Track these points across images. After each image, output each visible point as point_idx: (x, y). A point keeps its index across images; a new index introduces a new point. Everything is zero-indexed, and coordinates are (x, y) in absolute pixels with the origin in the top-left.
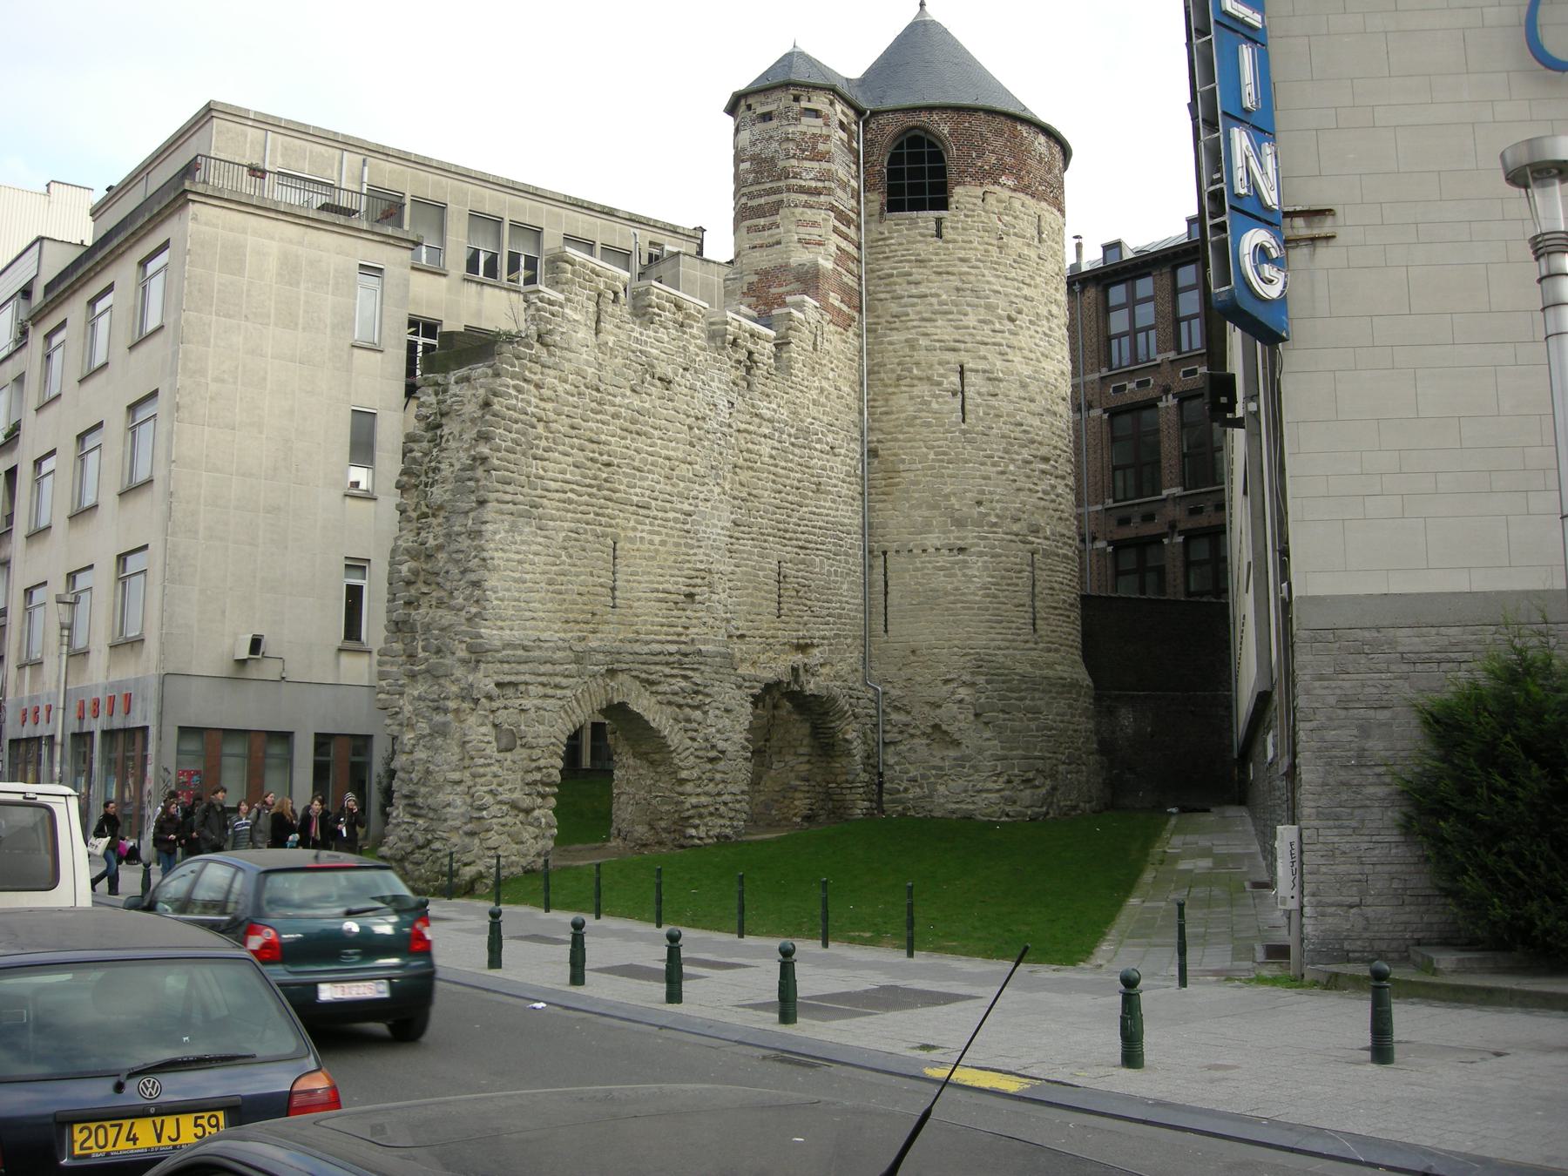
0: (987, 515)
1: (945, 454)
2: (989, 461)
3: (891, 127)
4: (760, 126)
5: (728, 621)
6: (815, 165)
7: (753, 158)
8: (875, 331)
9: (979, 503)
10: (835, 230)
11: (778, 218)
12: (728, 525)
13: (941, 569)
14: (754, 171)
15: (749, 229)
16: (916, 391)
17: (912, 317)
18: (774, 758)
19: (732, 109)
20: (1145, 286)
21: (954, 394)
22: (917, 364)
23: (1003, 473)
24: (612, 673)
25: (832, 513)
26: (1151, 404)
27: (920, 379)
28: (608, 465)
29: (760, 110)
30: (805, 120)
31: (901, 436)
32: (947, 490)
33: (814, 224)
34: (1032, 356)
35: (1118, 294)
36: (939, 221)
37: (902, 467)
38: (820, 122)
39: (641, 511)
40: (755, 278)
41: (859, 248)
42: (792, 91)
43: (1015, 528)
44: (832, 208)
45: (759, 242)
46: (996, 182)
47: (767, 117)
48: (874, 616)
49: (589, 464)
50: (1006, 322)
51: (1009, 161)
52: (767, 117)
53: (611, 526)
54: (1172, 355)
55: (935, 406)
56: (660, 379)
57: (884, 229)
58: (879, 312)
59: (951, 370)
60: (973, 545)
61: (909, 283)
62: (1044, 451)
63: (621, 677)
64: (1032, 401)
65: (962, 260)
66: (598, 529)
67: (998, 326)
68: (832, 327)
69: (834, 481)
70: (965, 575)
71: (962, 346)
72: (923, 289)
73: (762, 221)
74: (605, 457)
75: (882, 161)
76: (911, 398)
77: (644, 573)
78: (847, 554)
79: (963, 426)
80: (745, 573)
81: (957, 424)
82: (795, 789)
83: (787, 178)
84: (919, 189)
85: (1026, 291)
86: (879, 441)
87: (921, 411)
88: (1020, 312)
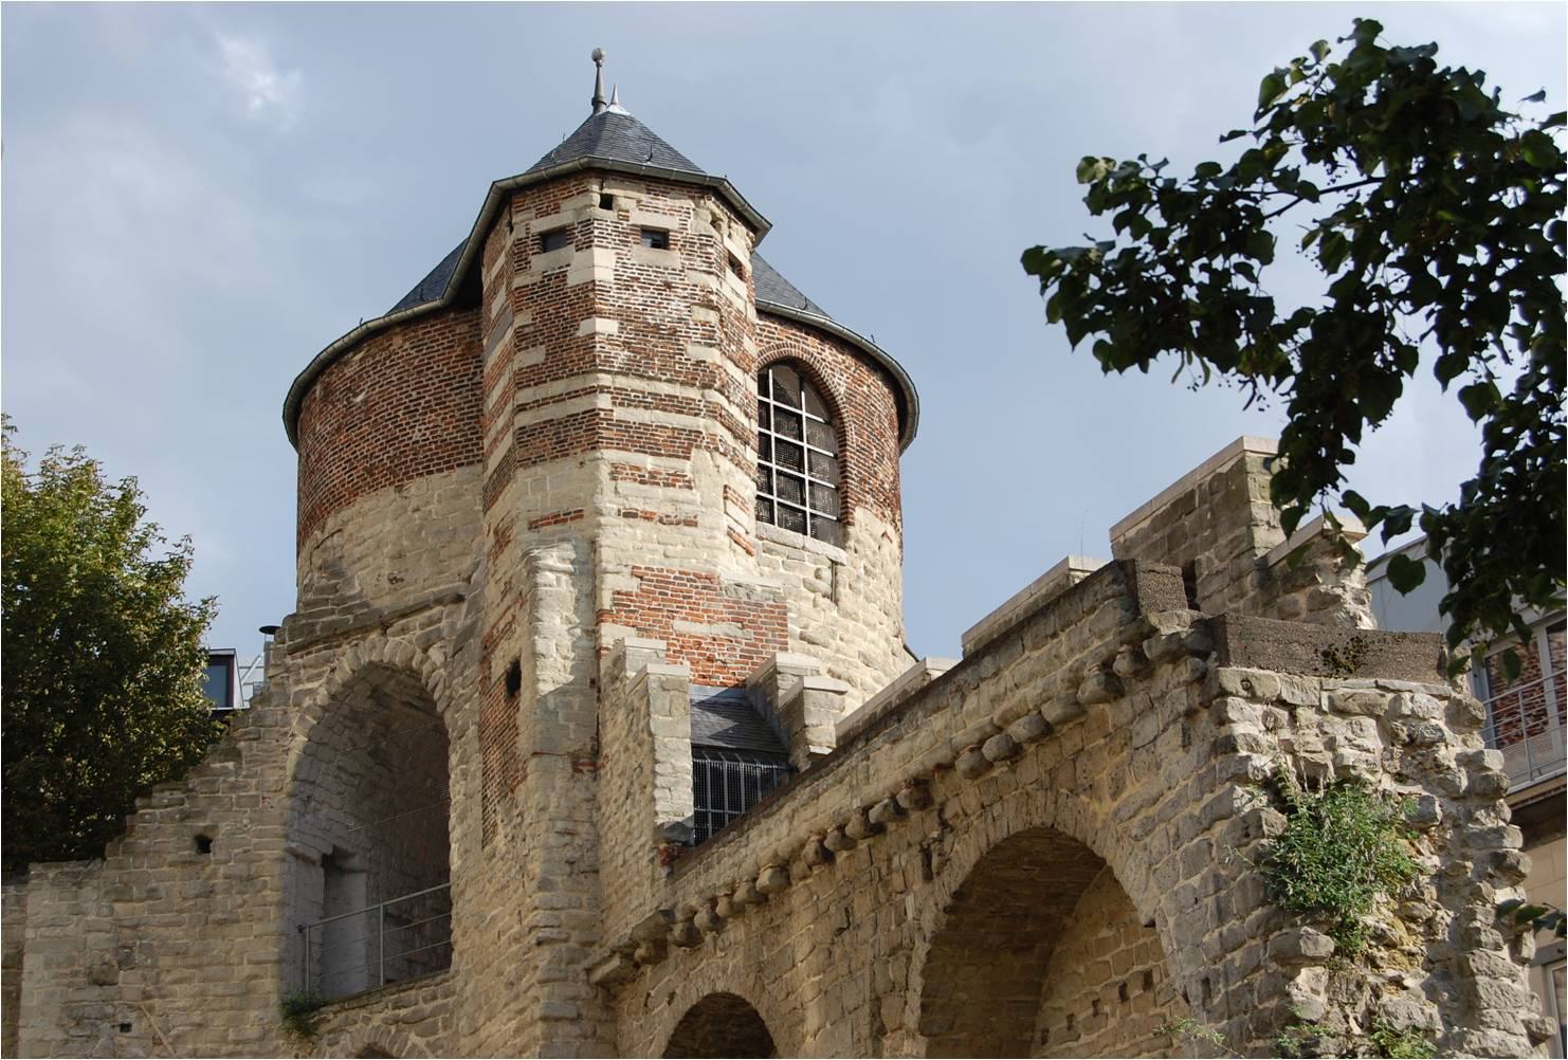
7: (624, 316)
11: (686, 467)
47: (660, 239)
52: (660, 239)
73: (649, 462)
83: (705, 386)
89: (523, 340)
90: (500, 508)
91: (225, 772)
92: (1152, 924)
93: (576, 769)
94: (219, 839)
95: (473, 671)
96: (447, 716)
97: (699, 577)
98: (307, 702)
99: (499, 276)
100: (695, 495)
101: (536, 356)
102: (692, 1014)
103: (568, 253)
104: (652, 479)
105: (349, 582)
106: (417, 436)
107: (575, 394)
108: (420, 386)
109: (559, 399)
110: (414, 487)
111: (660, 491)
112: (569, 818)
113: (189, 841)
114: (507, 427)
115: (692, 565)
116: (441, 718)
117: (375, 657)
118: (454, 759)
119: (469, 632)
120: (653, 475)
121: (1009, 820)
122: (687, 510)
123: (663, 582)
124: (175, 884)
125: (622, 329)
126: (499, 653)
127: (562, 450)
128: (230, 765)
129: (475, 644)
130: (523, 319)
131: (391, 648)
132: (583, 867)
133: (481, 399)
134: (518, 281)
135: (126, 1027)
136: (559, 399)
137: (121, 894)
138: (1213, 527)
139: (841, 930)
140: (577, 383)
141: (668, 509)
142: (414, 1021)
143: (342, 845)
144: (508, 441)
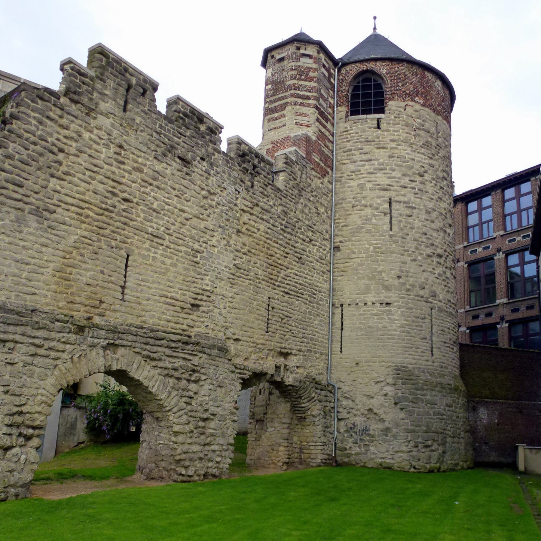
0: (404, 284)
1: (379, 248)
2: (406, 253)
3: (354, 70)
4: (277, 65)
5: (227, 328)
6: (308, 84)
8: (340, 181)
9: (399, 277)
10: (318, 120)
11: (284, 112)
12: (231, 266)
13: (375, 315)
14: (273, 89)
16: (363, 213)
17: (362, 172)
19: (264, 64)
20: (487, 201)
21: (385, 214)
22: (364, 198)
23: (415, 260)
24: (112, 346)
25: (309, 277)
26: (491, 258)
27: (366, 206)
28: (126, 200)
29: (278, 57)
30: (304, 60)
31: (354, 239)
32: (381, 268)
33: (305, 115)
34: (432, 197)
35: (473, 206)
36: (379, 120)
37: (353, 256)
38: (311, 61)
39: (156, 240)
41: (333, 136)
42: (296, 44)
43: (422, 293)
44: (317, 108)
46: (413, 100)
48: (334, 343)
49: (109, 195)
50: (418, 177)
51: (421, 90)
52: (282, 60)
53: (124, 242)
54: (502, 233)
55: (374, 221)
56: (179, 158)
57: (347, 125)
58: (343, 171)
59: (384, 201)
60: (395, 301)
61: (361, 154)
62: (439, 251)
63: (121, 351)
64: (433, 222)
65: (393, 141)
66: (113, 243)
67: (413, 179)
68: (314, 173)
69: (311, 259)
70: (390, 319)
71: (392, 188)
72: (368, 157)
73: (276, 115)
74: (125, 195)
75: (347, 89)
76: (360, 217)
77: (154, 282)
78: (318, 304)
79: (391, 233)
80: (242, 300)
81: (387, 231)
83: (291, 90)
84: (369, 103)
85: (431, 162)
86: (341, 242)
87: (364, 224)
88: (425, 172)
100: (287, 118)
111: (278, 121)
115: (285, 135)
122: (284, 122)
123: (277, 142)
141: (280, 125)
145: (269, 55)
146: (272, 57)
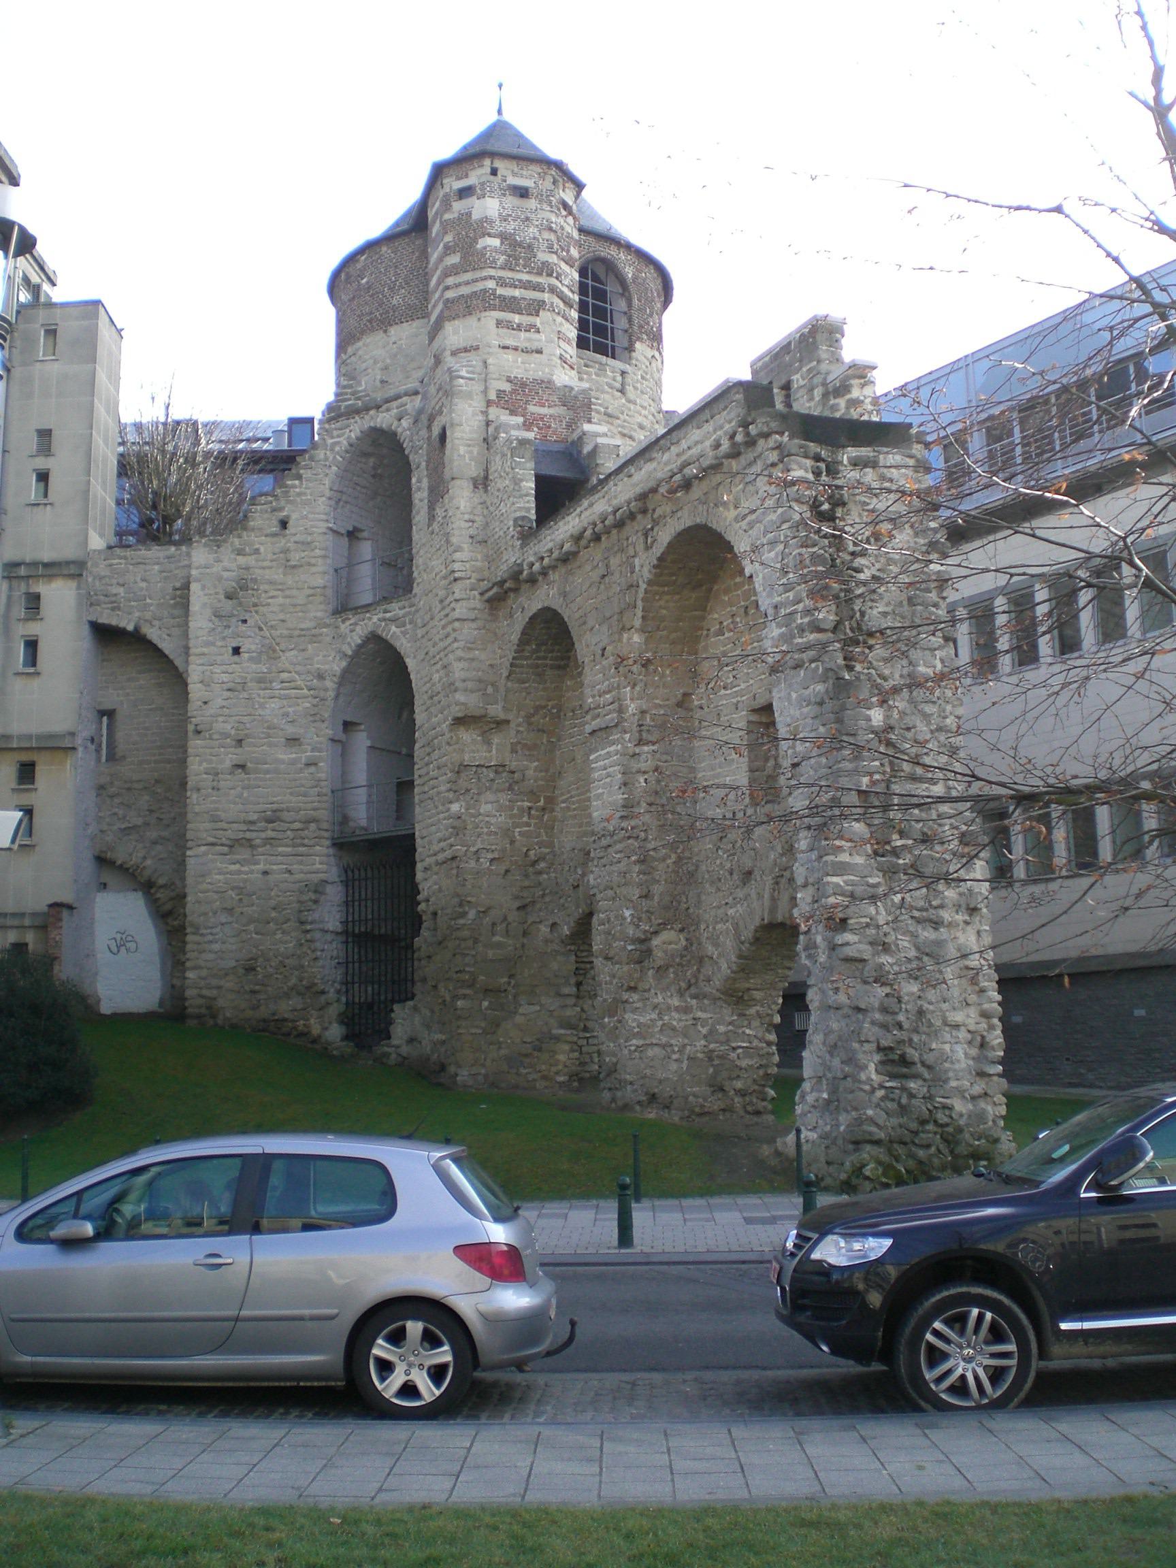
7: (503, 237)
11: (538, 321)
15: (499, 323)
18: (523, 999)
29: (513, 181)
40: (507, 387)
45: (510, 342)
52: (523, 193)
73: (517, 318)
82: (557, 1039)
83: (550, 275)
89: (448, 250)
90: (436, 344)
91: (294, 486)
92: (751, 577)
93: (476, 487)
94: (291, 523)
95: (424, 433)
96: (411, 458)
97: (543, 381)
98: (337, 449)
99: (436, 213)
100: (543, 337)
101: (454, 259)
102: (533, 618)
103: (473, 201)
104: (519, 328)
105: (359, 384)
106: (394, 302)
107: (476, 281)
108: (396, 274)
109: (467, 283)
110: (393, 331)
111: (523, 335)
112: (471, 513)
113: (275, 522)
114: (440, 298)
116: (407, 457)
117: (372, 424)
118: (414, 480)
119: (421, 411)
120: (519, 326)
121: (685, 520)
122: (535, 345)
123: (523, 385)
124: (267, 547)
125: (502, 243)
126: (436, 423)
127: (469, 312)
128: (297, 482)
129: (424, 418)
130: (448, 238)
131: (383, 419)
132: (479, 538)
133: (427, 285)
134: (447, 216)
135: (245, 621)
136: (467, 283)
137: (240, 552)
138: (801, 361)
139: (604, 576)
140: (478, 274)
142: (393, 620)
143: (356, 524)
144: (440, 306)
145: (487, 162)
146: (494, 172)
